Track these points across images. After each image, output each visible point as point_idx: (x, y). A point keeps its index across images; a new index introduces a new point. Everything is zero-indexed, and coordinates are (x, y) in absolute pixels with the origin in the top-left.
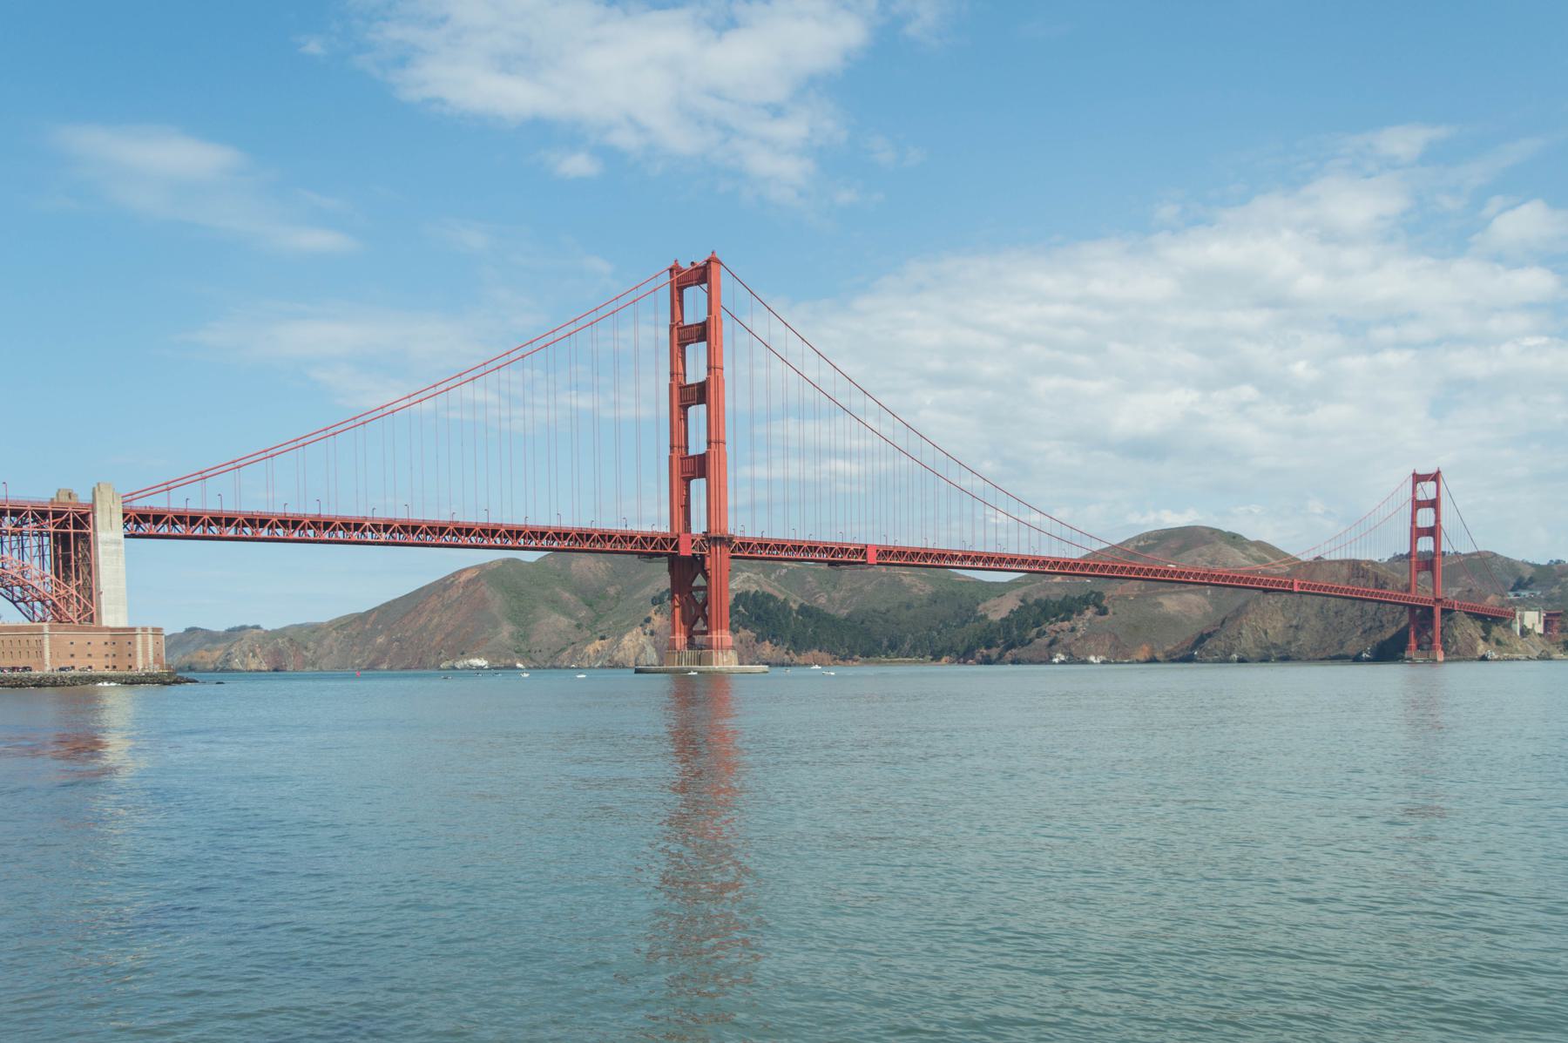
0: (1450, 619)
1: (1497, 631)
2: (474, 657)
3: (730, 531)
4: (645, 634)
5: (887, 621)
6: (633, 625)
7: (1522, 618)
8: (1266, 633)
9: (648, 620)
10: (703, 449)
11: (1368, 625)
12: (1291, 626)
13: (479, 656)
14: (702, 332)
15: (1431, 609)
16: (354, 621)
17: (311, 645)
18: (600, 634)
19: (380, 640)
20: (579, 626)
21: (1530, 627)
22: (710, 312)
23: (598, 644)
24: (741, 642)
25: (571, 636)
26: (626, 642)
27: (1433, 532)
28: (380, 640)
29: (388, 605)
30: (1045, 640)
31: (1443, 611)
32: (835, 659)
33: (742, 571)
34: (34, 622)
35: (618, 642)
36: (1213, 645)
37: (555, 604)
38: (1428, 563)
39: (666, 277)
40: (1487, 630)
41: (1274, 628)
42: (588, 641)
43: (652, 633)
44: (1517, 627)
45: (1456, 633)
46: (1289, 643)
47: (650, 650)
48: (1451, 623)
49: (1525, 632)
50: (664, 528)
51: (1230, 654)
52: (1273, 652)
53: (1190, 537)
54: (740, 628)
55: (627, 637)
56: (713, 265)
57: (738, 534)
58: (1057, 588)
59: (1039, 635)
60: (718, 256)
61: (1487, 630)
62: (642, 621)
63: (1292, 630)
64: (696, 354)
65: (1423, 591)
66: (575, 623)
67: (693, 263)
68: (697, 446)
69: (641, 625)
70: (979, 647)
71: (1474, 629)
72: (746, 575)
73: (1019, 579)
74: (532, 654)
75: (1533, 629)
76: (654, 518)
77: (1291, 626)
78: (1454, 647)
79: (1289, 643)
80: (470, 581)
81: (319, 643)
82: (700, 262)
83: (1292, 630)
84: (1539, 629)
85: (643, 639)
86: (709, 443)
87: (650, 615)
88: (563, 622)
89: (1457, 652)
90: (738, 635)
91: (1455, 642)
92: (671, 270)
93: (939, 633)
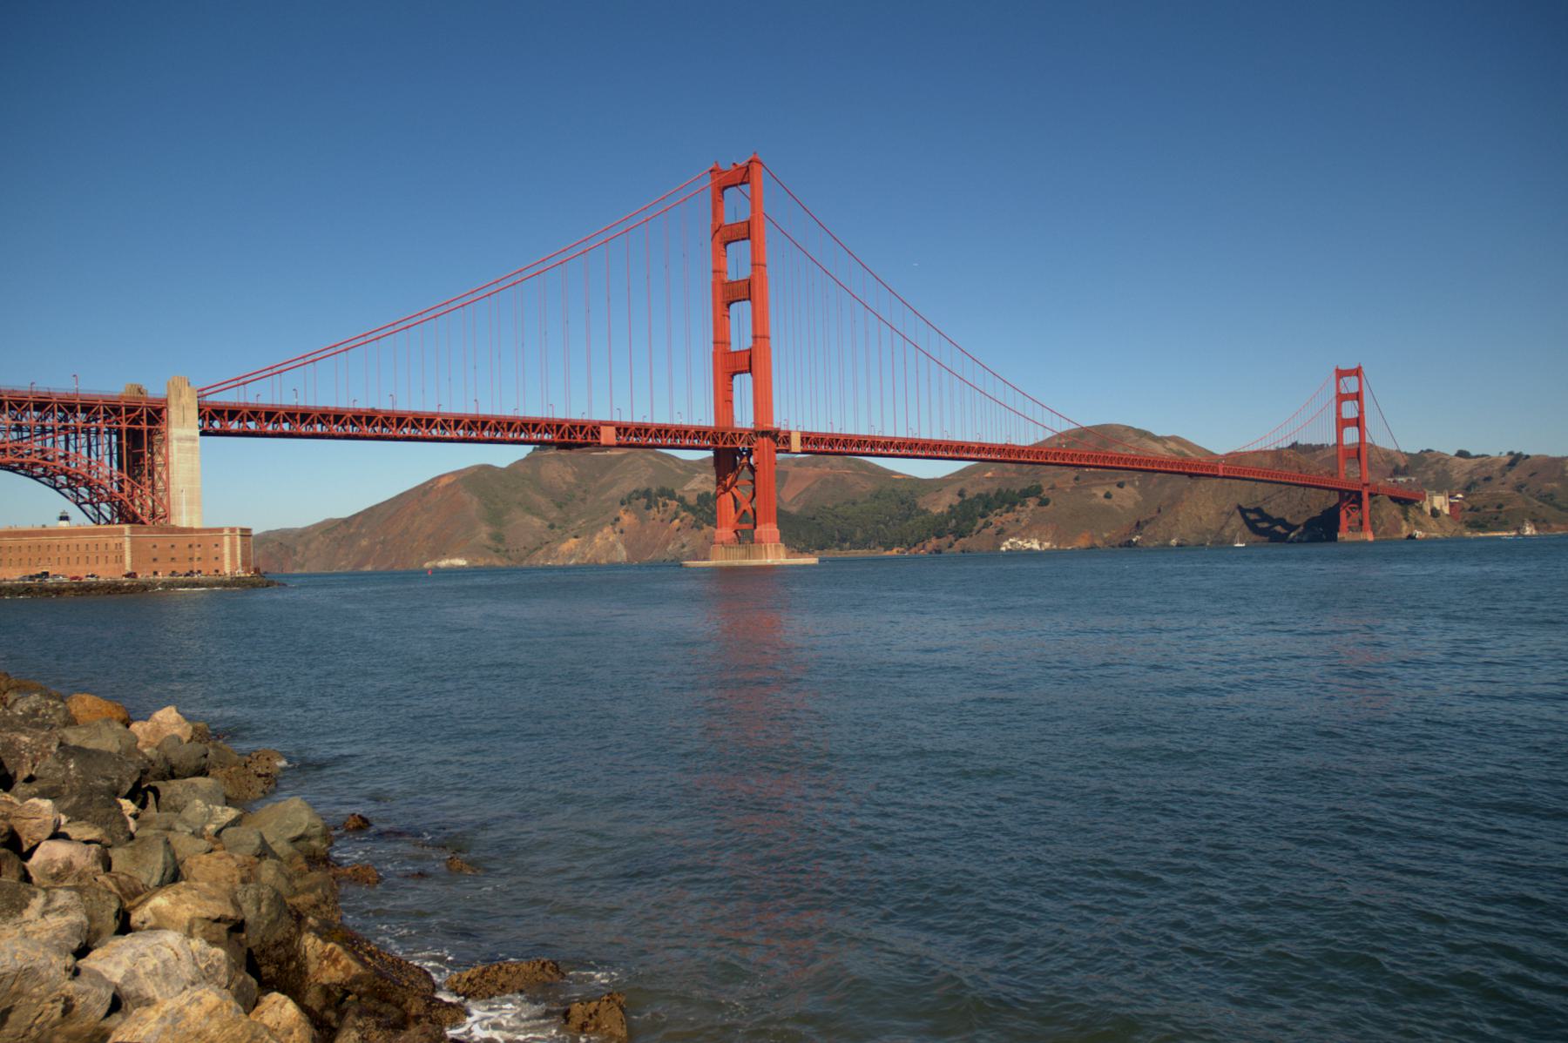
0: (1376, 502)
1: (1412, 512)
4: (615, 533)
6: (604, 524)
7: (1431, 502)
8: (1200, 519)
9: (618, 519)
11: (1296, 509)
12: (1223, 513)
13: (460, 556)
15: (1359, 494)
16: (339, 525)
17: (299, 548)
18: (573, 533)
19: (364, 543)
20: (552, 526)
21: (1438, 508)
24: (706, 538)
25: (545, 536)
26: (597, 540)
27: (1358, 422)
28: (364, 543)
29: (371, 509)
30: (991, 530)
31: (1371, 495)
32: (793, 552)
33: (700, 473)
34: (99, 524)
35: (591, 541)
36: (1153, 532)
37: (531, 509)
40: (1405, 513)
41: (1208, 514)
42: (563, 540)
43: (622, 532)
44: (1427, 508)
45: (1383, 514)
46: (1222, 528)
47: (620, 547)
48: (1376, 506)
51: (1170, 539)
52: (1209, 537)
54: (705, 525)
55: (599, 535)
58: (1018, 478)
59: (987, 525)
61: (1405, 513)
62: (613, 520)
65: (1350, 474)
66: (547, 523)
70: (928, 537)
71: (1395, 509)
72: (703, 476)
73: (961, 472)
74: (511, 553)
75: (1441, 510)
77: (1223, 513)
78: (1382, 528)
79: (1222, 528)
80: (448, 486)
81: (307, 545)
84: (1446, 510)
87: (618, 515)
88: (537, 522)
89: (1385, 533)
91: (1382, 524)
93: (886, 525)
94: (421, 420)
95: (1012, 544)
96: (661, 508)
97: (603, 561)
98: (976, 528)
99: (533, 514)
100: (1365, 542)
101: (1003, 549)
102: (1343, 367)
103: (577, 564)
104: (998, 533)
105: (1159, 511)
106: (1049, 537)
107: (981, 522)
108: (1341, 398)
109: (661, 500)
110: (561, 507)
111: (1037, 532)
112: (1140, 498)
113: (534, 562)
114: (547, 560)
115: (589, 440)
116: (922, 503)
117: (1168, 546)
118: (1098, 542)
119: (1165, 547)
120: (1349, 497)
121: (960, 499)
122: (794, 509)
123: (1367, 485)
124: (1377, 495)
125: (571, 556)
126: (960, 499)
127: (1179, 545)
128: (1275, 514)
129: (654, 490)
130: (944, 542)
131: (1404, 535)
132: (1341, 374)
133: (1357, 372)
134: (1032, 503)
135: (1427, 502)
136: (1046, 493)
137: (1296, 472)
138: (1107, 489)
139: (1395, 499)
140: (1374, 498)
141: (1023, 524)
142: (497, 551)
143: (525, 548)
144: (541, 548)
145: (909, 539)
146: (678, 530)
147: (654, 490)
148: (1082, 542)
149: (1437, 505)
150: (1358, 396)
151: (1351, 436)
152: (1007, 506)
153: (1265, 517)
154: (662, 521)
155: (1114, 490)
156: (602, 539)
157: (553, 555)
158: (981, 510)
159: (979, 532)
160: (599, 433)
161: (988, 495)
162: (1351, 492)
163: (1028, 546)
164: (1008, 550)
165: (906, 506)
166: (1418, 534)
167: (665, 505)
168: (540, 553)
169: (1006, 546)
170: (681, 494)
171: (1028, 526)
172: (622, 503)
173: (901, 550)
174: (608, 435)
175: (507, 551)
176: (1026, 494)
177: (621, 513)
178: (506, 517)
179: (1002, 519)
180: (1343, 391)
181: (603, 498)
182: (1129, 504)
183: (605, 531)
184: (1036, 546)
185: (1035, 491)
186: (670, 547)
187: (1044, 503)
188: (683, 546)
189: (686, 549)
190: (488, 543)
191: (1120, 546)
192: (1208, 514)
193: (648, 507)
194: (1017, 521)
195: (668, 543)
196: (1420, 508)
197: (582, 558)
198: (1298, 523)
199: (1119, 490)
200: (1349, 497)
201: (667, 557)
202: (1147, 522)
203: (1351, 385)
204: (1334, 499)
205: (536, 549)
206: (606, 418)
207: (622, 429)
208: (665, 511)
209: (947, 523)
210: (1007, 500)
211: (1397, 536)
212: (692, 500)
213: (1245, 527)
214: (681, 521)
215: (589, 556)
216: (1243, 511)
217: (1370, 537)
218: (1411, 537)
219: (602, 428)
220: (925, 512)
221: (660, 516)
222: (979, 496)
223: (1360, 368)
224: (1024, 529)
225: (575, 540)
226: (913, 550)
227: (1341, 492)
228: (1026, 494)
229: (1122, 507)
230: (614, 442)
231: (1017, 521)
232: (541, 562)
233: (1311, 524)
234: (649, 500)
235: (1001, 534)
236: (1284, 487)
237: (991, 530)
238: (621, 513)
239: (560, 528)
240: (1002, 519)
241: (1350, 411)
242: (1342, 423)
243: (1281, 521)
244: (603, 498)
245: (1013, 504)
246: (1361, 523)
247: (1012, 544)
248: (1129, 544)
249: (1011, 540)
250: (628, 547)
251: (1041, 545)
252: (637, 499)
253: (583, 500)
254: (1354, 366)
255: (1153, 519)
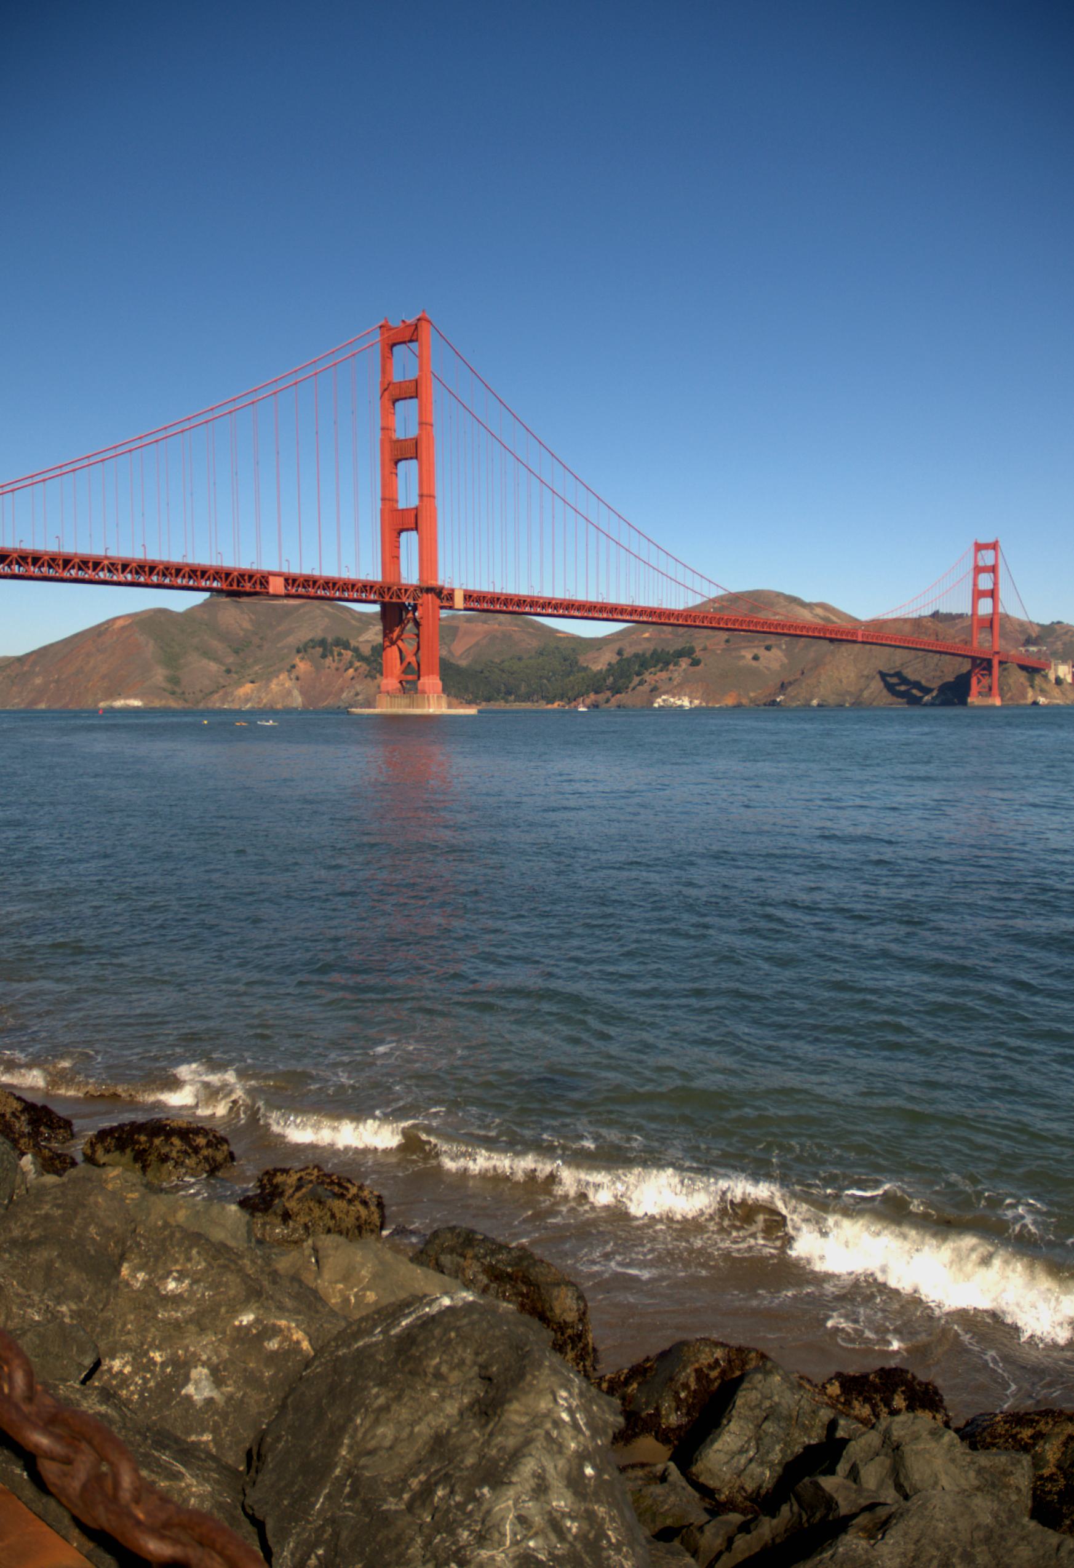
0: (1005, 669)
1: (1038, 680)
2: (128, 697)
3: (440, 583)
5: (503, 671)
6: (280, 671)
7: (1056, 670)
8: (841, 681)
9: (294, 667)
10: (414, 502)
13: (135, 697)
14: (412, 391)
18: (250, 678)
20: (229, 671)
21: (1062, 676)
22: (421, 369)
23: (248, 687)
25: (221, 680)
27: (993, 594)
31: (1001, 663)
38: (989, 623)
39: (377, 337)
41: (848, 677)
42: (239, 684)
43: (297, 679)
45: (1011, 681)
46: (862, 691)
47: (296, 693)
48: (1005, 673)
49: (1059, 681)
50: (380, 579)
51: (811, 700)
53: (757, 599)
55: (275, 681)
56: (424, 323)
57: (447, 586)
58: (672, 639)
59: (641, 683)
60: (428, 316)
63: (863, 680)
64: (407, 410)
65: (982, 643)
66: (224, 668)
67: (403, 321)
68: (408, 498)
69: (289, 671)
70: (587, 693)
71: (1021, 677)
76: (371, 571)
78: (1009, 695)
79: (862, 691)
82: (411, 320)
83: (863, 680)
84: (1069, 679)
85: (288, 684)
86: (421, 496)
88: (213, 666)
89: (1011, 699)
90: (376, 681)
91: (1010, 690)
92: (381, 327)
93: (549, 680)
94: (27, 558)
95: (664, 701)
96: (336, 658)
97: (279, 706)
98: (632, 685)
99: (209, 658)
100: (993, 707)
101: (656, 705)
102: (982, 541)
103: (253, 707)
104: (652, 691)
105: (803, 673)
106: (699, 695)
107: (636, 680)
108: (978, 570)
109: (336, 650)
110: (236, 652)
111: (688, 691)
112: (786, 661)
113: (210, 705)
114: (223, 704)
115: (258, 589)
116: (583, 661)
117: (809, 706)
118: (745, 701)
119: (807, 706)
120: (981, 664)
121: (618, 658)
122: (463, 663)
123: (997, 653)
124: (1006, 663)
125: (247, 701)
126: (618, 658)
127: (819, 705)
128: (912, 677)
129: (330, 640)
130: (601, 697)
131: (1030, 701)
132: (979, 547)
133: (994, 546)
134: (684, 663)
135: (1052, 671)
136: (698, 654)
137: (933, 638)
138: (755, 651)
139: (1023, 667)
140: (1004, 666)
141: (675, 683)
142: (173, 693)
143: (201, 691)
144: (217, 692)
145: (570, 694)
146: (352, 679)
147: (330, 640)
148: (730, 701)
149: (1061, 674)
150: (993, 569)
151: (985, 607)
152: (661, 665)
153: (904, 680)
154: (337, 669)
155: (762, 652)
156: (277, 684)
157: (230, 699)
158: (637, 668)
159: (634, 689)
160: (267, 582)
161: (644, 655)
162: (983, 660)
163: (679, 703)
164: (660, 707)
165: (568, 663)
166: (1042, 700)
167: (340, 654)
168: (216, 696)
169: (658, 702)
170: (356, 644)
171: (680, 685)
172: (298, 651)
173: (561, 703)
174: (276, 586)
175: (183, 693)
176: (680, 654)
177: (297, 661)
178: (182, 661)
179: (656, 677)
180: (981, 564)
181: (279, 645)
182: (775, 666)
183: (281, 677)
184: (686, 703)
185: (687, 652)
186: (344, 695)
187: (696, 663)
188: (357, 694)
189: (360, 697)
190: (164, 685)
191: (765, 705)
192: (848, 677)
193: (324, 656)
194: (670, 679)
195: (342, 690)
196: (1046, 677)
197: (259, 703)
198: (933, 686)
199: (767, 653)
200: (981, 664)
201: (341, 704)
202: (790, 683)
203: (988, 558)
204: (966, 666)
205: (212, 693)
206: (275, 568)
207: (291, 580)
208: (340, 660)
209: (605, 680)
210: (662, 659)
211: (1022, 702)
212: (366, 650)
213: (885, 692)
214: (356, 670)
215: (265, 701)
216: (883, 676)
217: (998, 702)
218: (1035, 703)
219: (271, 579)
220: (585, 669)
221: (334, 665)
222: (636, 656)
223: (997, 542)
224: (675, 687)
225: (251, 685)
226: (573, 705)
227: (974, 659)
228: (680, 654)
229: (768, 669)
230: (282, 590)
231: (670, 679)
232: (218, 705)
233: (945, 688)
234: (325, 649)
235: (655, 691)
236: (920, 654)
237: (646, 688)
238: (297, 661)
239: (236, 673)
240: (656, 677)
241: (985, 582)
242: (978, 594)
243: (917, 685)
244: (279, 645)
245: (667, 664)
246: (990, 689)
247: (664, 701)
248: (773, 703)
249: (664, 697)
250: (302, 693)
251: (691, 702)
252: (313, 647)
253: (260, 647)
254: (991, 540)
255: (796, 680)
